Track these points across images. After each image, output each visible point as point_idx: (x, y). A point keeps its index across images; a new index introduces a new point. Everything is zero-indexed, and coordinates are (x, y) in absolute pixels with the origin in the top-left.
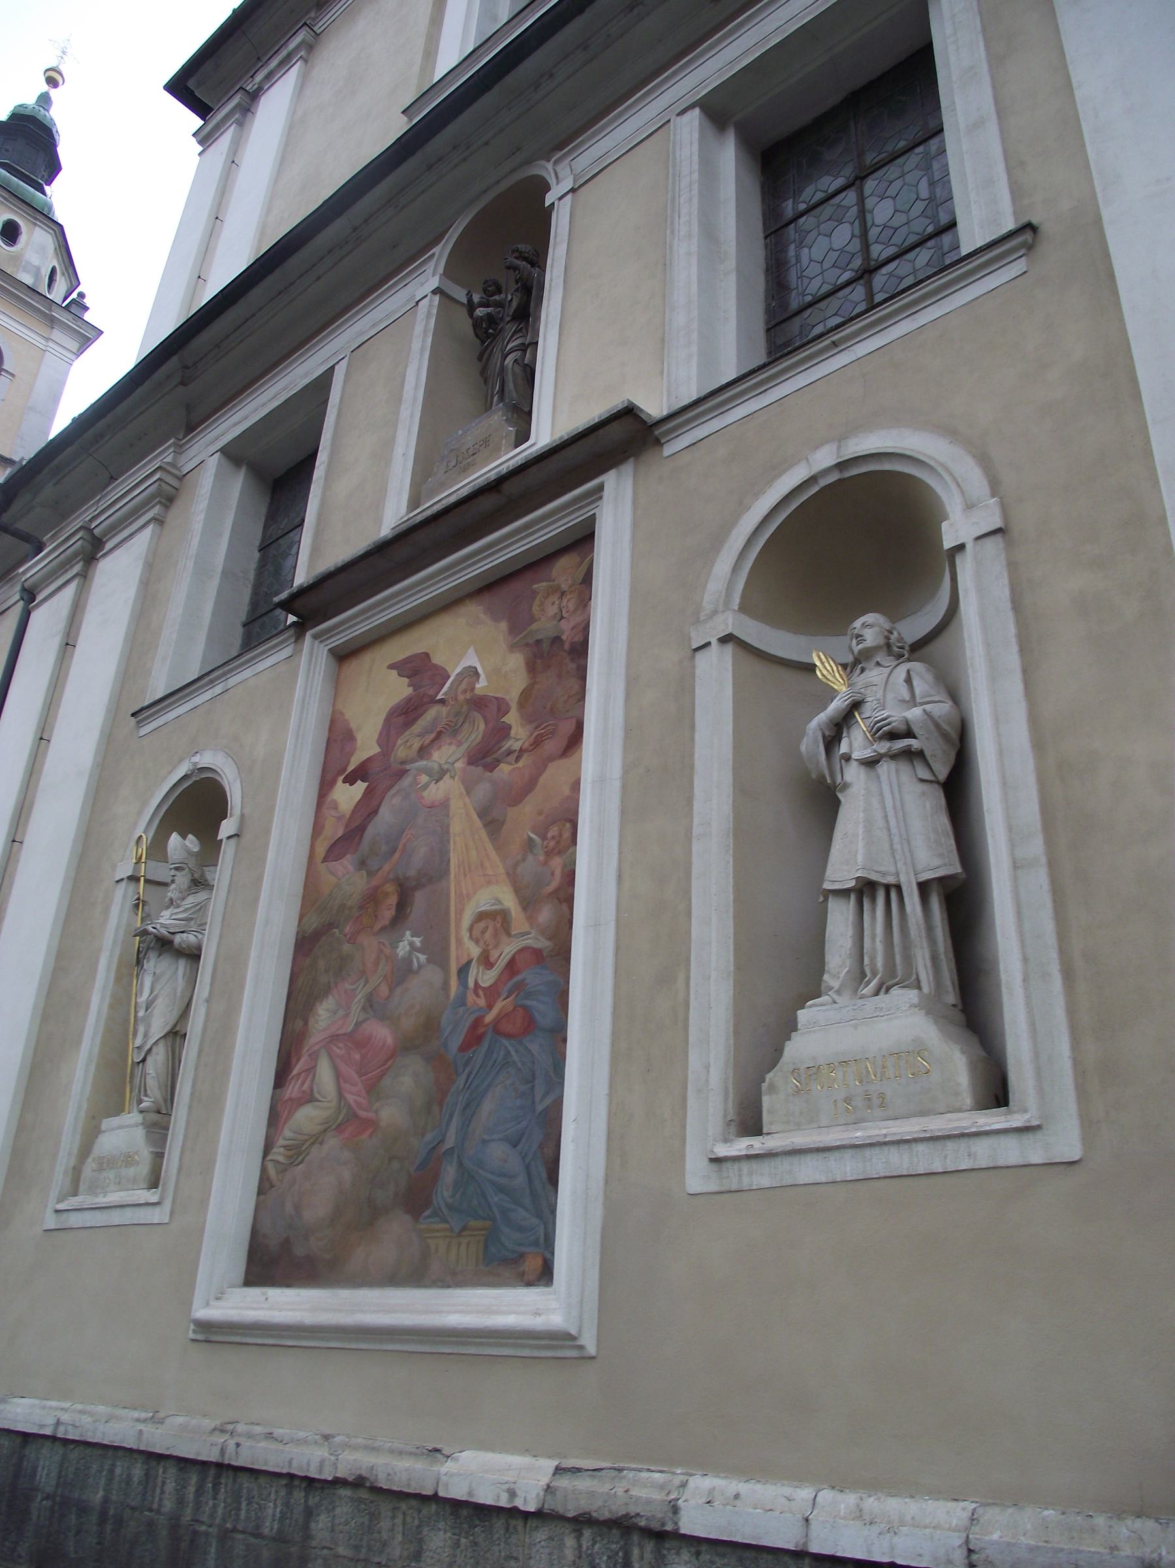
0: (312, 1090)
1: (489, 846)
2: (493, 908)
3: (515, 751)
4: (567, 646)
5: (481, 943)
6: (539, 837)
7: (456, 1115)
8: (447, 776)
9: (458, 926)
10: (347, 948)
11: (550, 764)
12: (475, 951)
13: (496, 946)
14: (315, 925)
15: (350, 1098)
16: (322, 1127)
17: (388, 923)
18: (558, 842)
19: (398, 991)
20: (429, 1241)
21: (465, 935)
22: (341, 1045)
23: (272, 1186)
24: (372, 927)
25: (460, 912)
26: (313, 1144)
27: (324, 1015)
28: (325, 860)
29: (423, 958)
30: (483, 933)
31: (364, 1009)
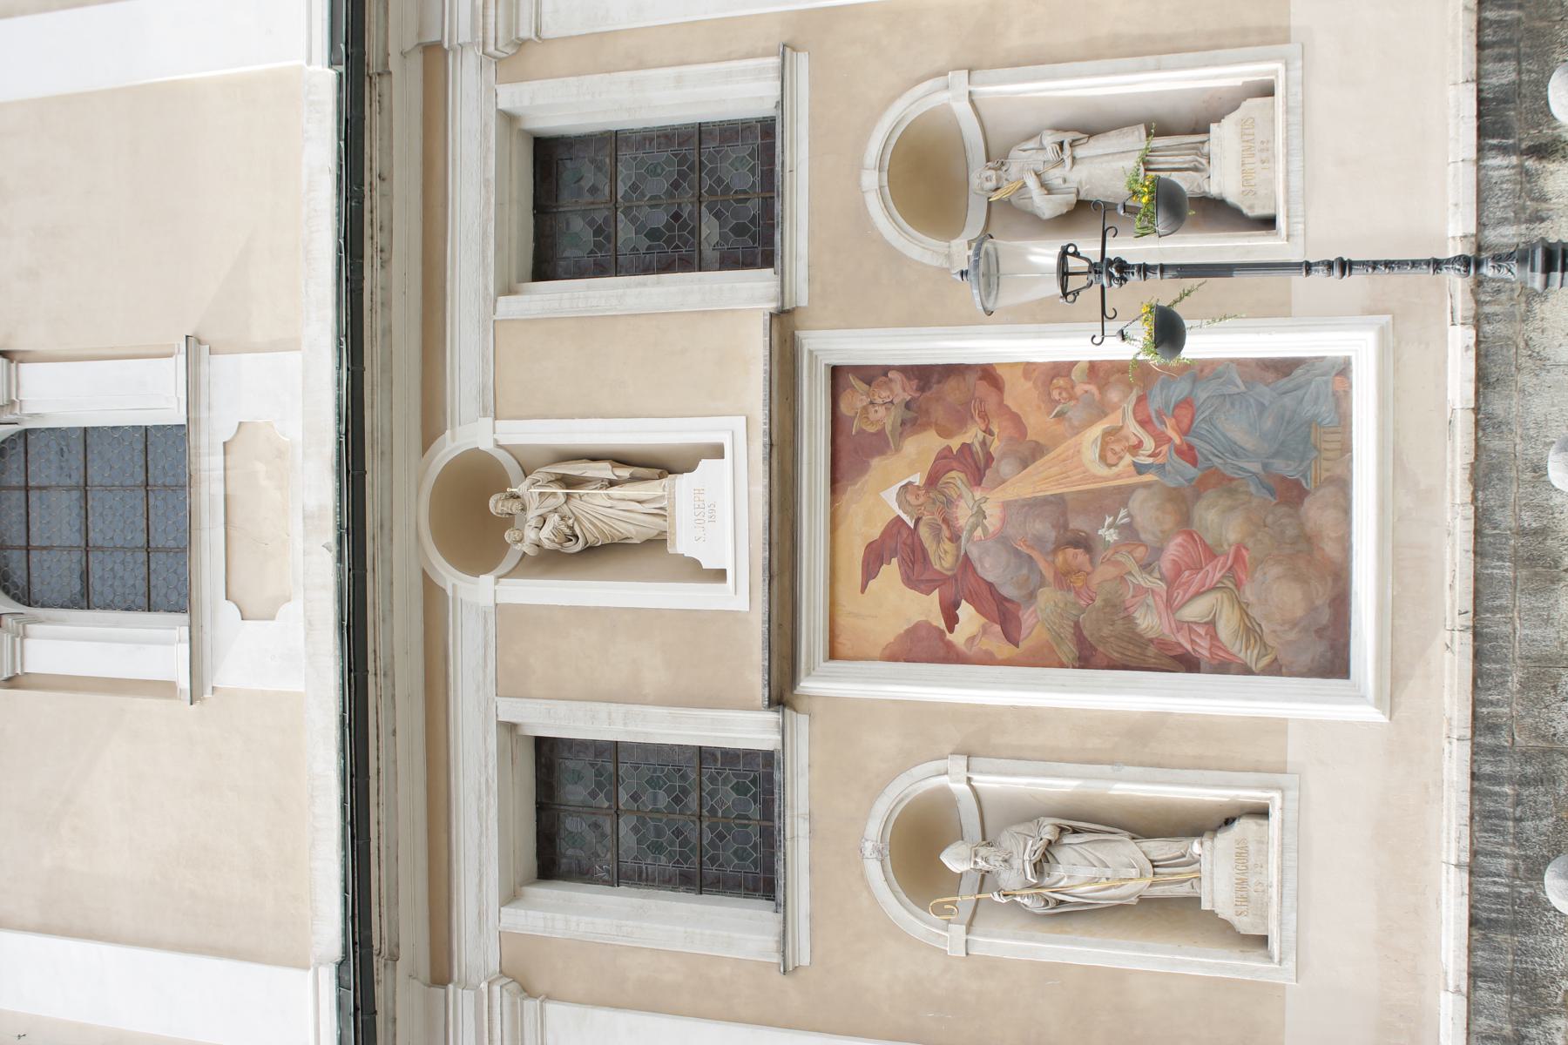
0: (1206, 623)
1: (1053, 454)
2: (1099, 443)
3: (984, 436)
4: (917, 395)
5: (1122, 454)
6: (1056, 407)
7: (1240, 464)
8: (984, 507)
9: (1105, 479)
10: (1098, 602)
11: (1005, 402)
12: (1128, 459)
13: (1127, 439)
14: (1070, 645)
15: (1218, 575)
16: (1236, 606)
17: (1087, 556)
18: (1065, 389)
19: (1143, 536)
20: (1322, 478)
21: (1115, 470)
22: (1175, 595)
23: (1276, 659)
24: (1088, 574)
25: (1096, 478)
26: (1247, 615)
27: (1149, 622)
28: (1017, 646)
29: (1123, 513)
30: (1115, 454)
31: (1150, 574)
